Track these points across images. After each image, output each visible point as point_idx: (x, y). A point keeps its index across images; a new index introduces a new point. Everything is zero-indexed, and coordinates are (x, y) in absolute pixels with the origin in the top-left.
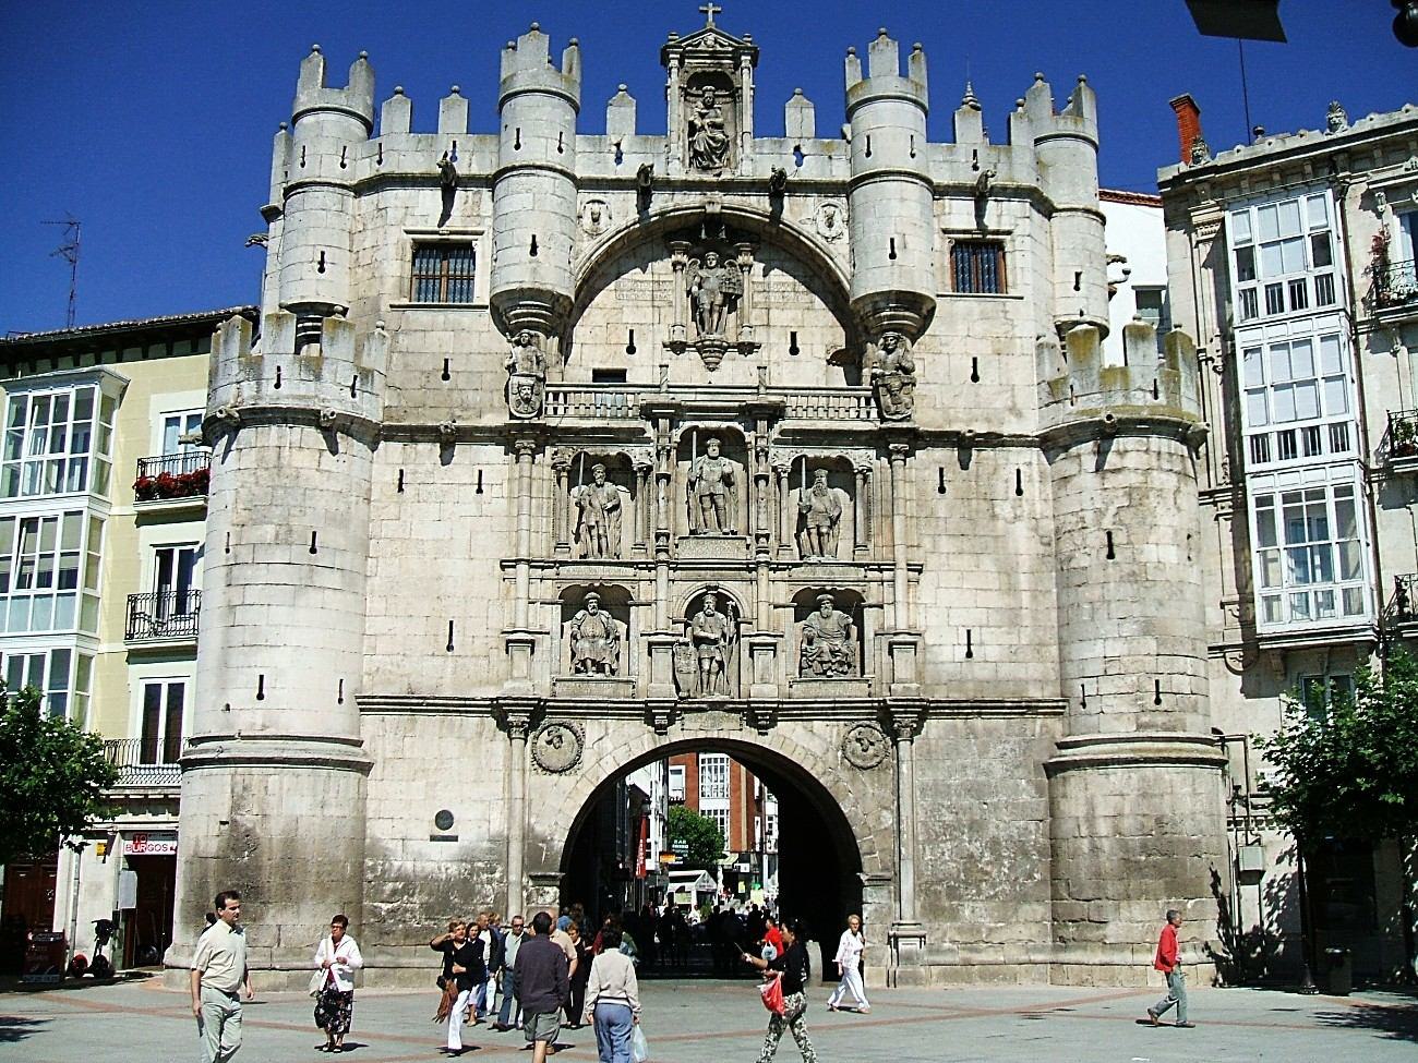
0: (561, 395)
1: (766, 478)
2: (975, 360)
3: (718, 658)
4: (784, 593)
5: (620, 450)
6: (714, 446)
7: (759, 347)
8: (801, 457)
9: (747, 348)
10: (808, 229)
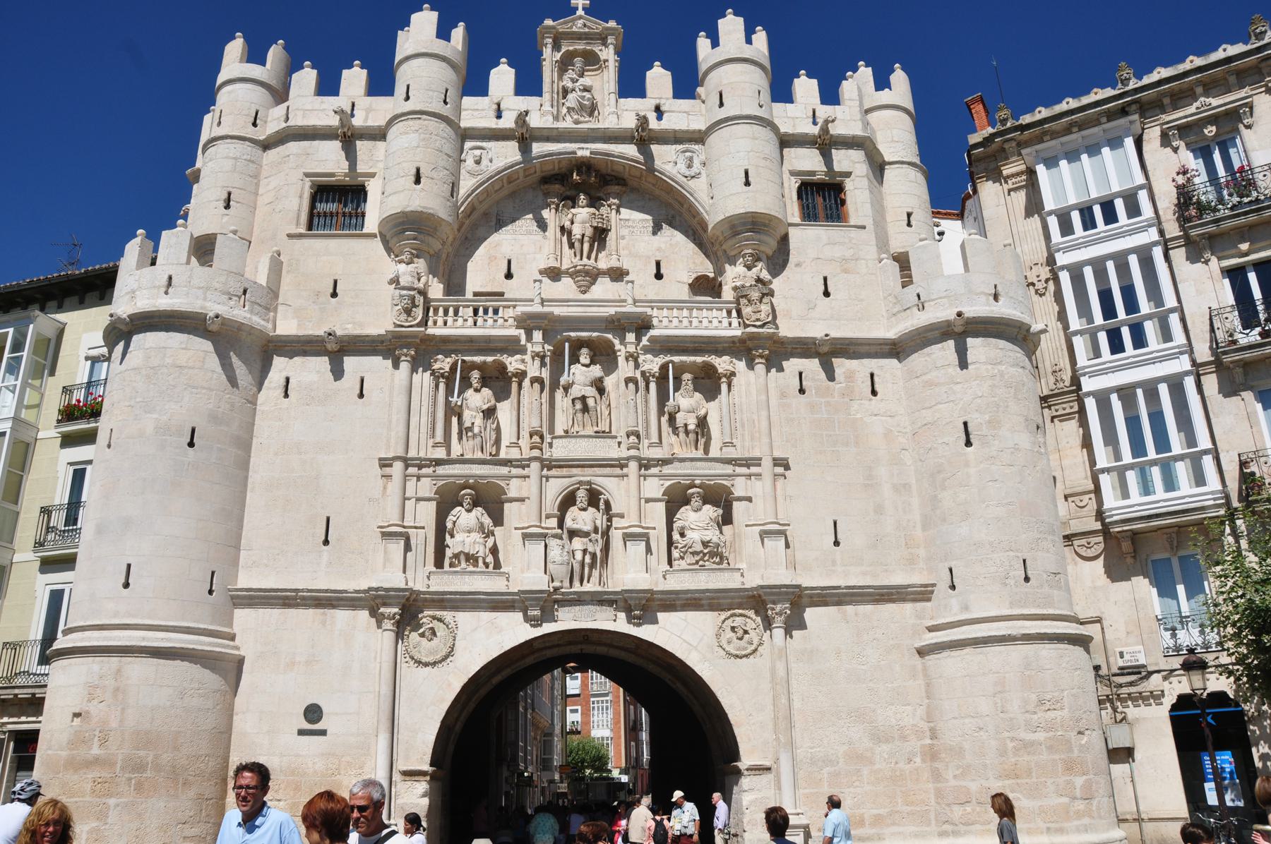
0: (441, 310)
2: (825, 279)
3: (591, 549)
4: (654, 487)
9: (618, 275)
10: (669, 169)
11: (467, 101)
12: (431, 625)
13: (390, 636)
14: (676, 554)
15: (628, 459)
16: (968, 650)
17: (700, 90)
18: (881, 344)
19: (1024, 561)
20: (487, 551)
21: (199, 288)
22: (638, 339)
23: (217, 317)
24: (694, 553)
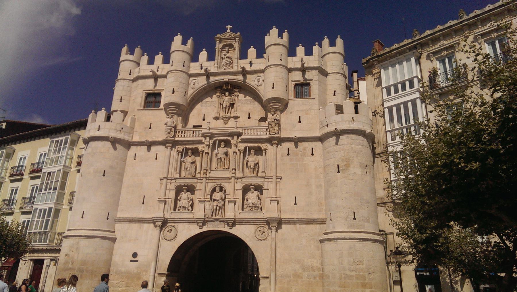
0: (180, 132)
1: (236, 153)
2: (300, 117)
5: (196, 146)
6: (223, 145)
7: (239, 117)
8: (247, 146)
9: (236, 118)
11: (192, 64)
12: (170, 228)
13: (159, 231)
14: (245, 207)
15: (232, 177)
16: (332, 242)
17: (264, 55)
18: (316, 138)
19: (354, 213)
20: (189, 205)
21: (108, 129)
22: (238, 138)
23: (112, 138)
24: (250, 207)
